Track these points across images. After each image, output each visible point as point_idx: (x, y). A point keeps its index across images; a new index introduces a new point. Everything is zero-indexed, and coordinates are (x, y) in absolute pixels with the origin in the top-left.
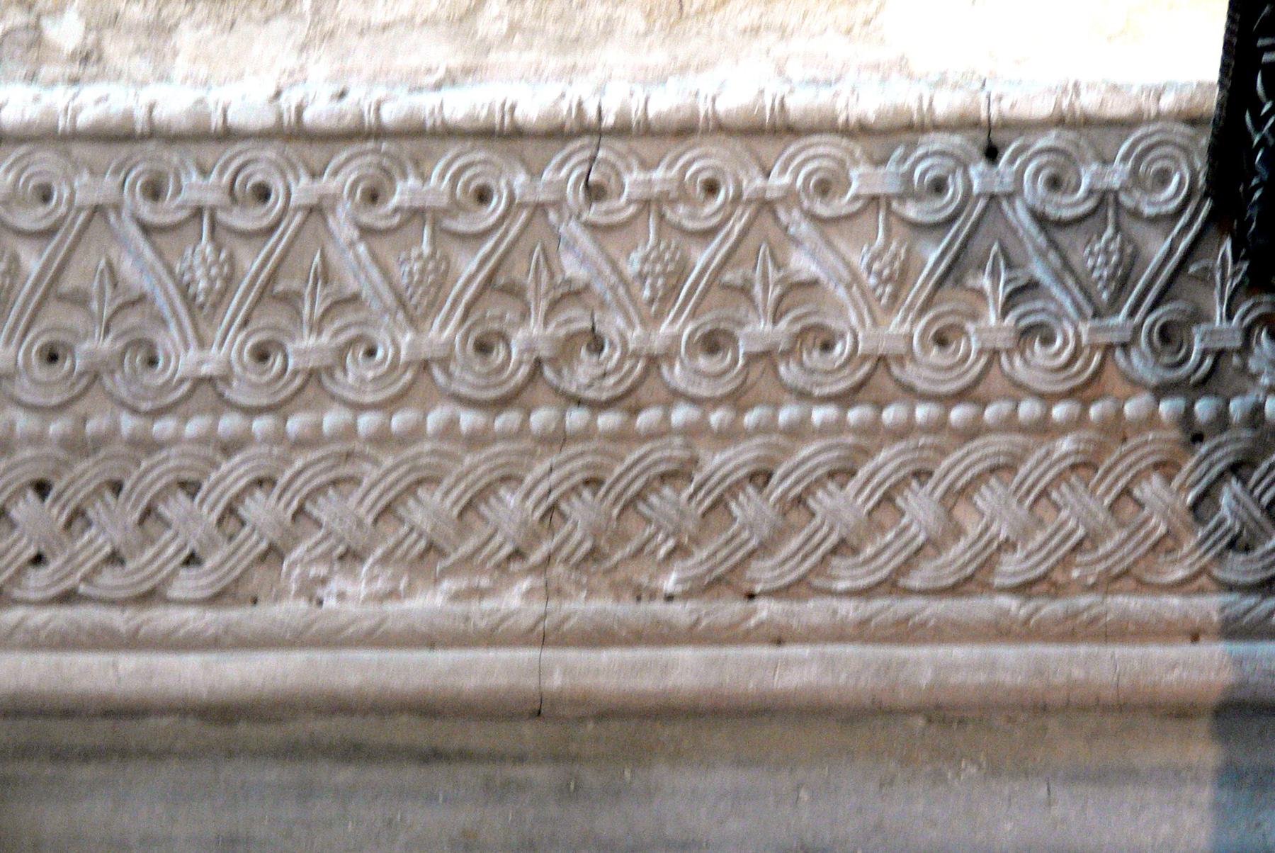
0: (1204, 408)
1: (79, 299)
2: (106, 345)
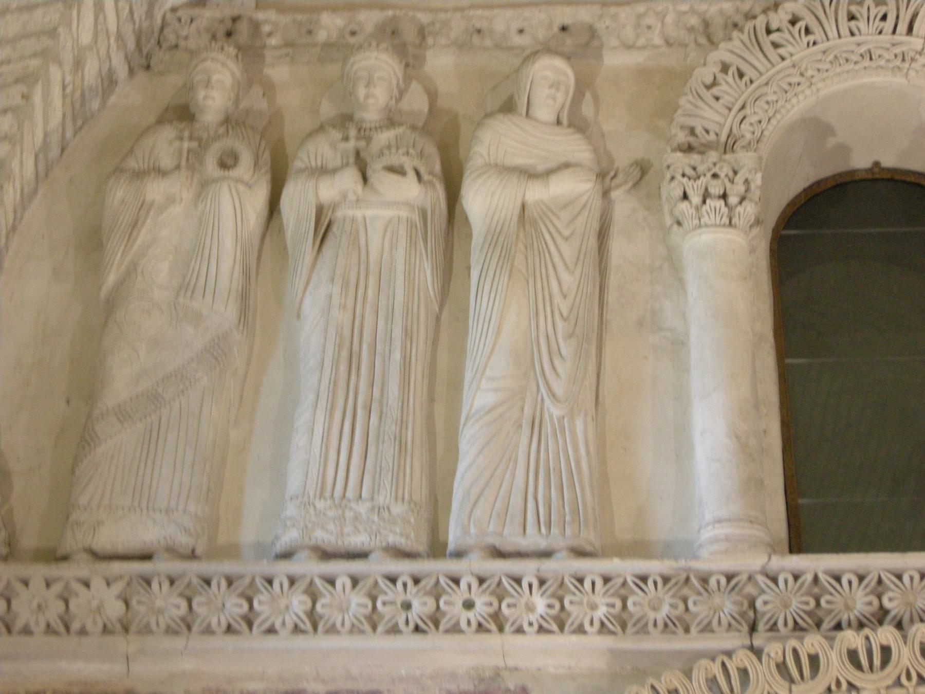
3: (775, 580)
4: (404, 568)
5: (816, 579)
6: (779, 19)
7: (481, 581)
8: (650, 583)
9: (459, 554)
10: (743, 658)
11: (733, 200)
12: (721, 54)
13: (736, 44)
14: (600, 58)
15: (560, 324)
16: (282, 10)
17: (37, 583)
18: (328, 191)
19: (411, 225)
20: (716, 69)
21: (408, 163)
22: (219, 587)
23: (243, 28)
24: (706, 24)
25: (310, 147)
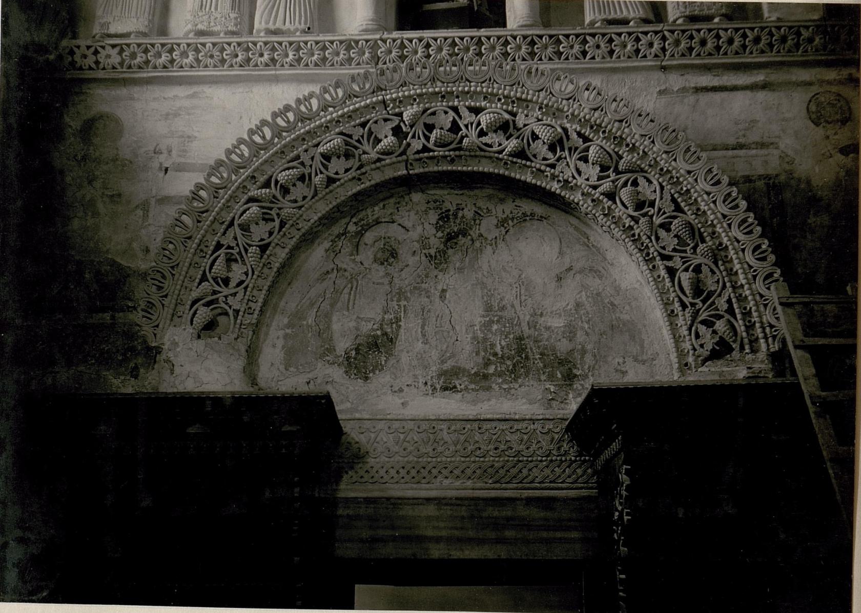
0: (563, 459)
1: (408, 442)
2: (412, 448)
8: (335, 44)
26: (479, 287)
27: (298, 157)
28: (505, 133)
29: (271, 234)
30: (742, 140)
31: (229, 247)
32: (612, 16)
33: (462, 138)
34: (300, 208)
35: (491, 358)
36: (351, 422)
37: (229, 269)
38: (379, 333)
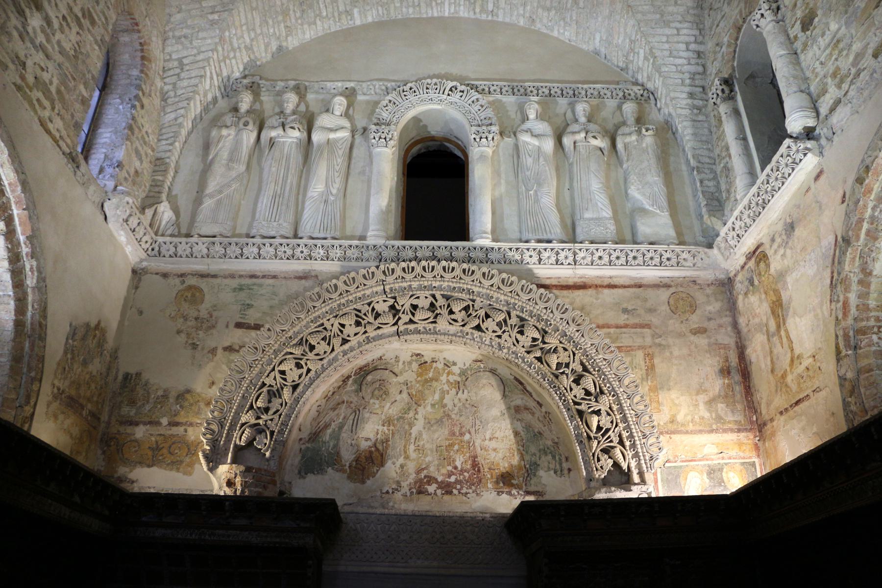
3: (387, 247)
4: (284, 241)
5: (398, 247)
6: (407, 88)
7: (306, 245)
9: (301, 238)
10: (373, 269)
11: (388, 139)
12: (389, 97)
13: (394, 95)
14: (356, 97)
15: (336, 173)
16: (267, 80)
17: (184, 243)
18: (273, 134)
19: (297, 144)
20: (387, 102)
21: (296, 126)
22: (233, 247)
23: (255, 85)
24: (387, 88)
25: (270, 120)
26: (446, 418)
27: (322, 324)
28: (467, 313)
29: (300, 377)
30: (627, 322)
31: (270, 386)
32: (541, 237)
33: (437, 315)
34: (321, 360)
35: (453, 470)
36: (351, 515)
37: (270, 401)
38: (373, 449)
